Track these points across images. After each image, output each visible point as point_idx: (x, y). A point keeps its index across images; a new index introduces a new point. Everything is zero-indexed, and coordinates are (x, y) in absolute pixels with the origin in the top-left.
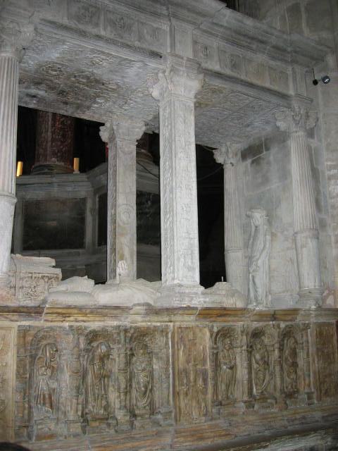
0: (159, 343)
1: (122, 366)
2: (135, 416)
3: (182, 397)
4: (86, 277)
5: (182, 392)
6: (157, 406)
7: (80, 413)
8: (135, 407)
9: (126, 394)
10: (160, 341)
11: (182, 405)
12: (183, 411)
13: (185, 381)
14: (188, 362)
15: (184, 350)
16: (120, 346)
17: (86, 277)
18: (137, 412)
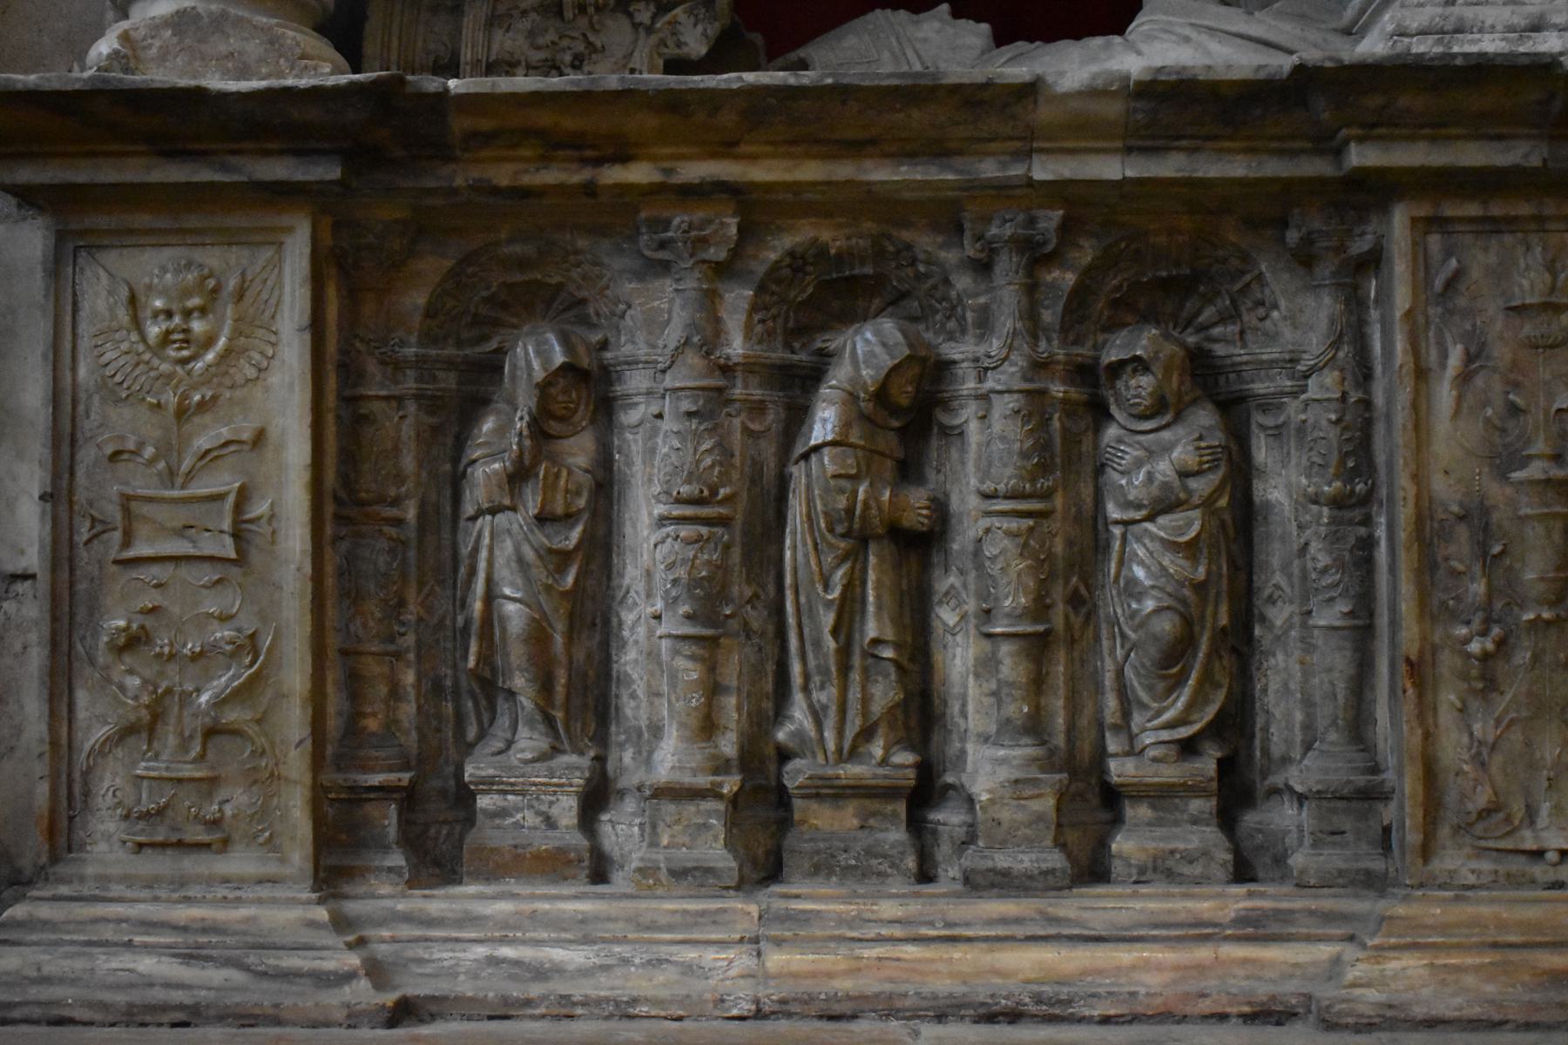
0: (1288, 334)
1: (1006, 476)
2: (1112, 798)
3: (1449, 697)
4: (945, 7)
5: (1448, 662)
6: (1277, 750)
7: (728, 745)
8: (1113, 745)
9: (1038, 646)
10: (1292, 319)
11: (1453, 747)
12: (1451, 798)
13: (1478, 588)
14: (1504, 460)
15: (1464, 378)
16: (995, 346)
17: (945, 7)
18: (1120, 770)
